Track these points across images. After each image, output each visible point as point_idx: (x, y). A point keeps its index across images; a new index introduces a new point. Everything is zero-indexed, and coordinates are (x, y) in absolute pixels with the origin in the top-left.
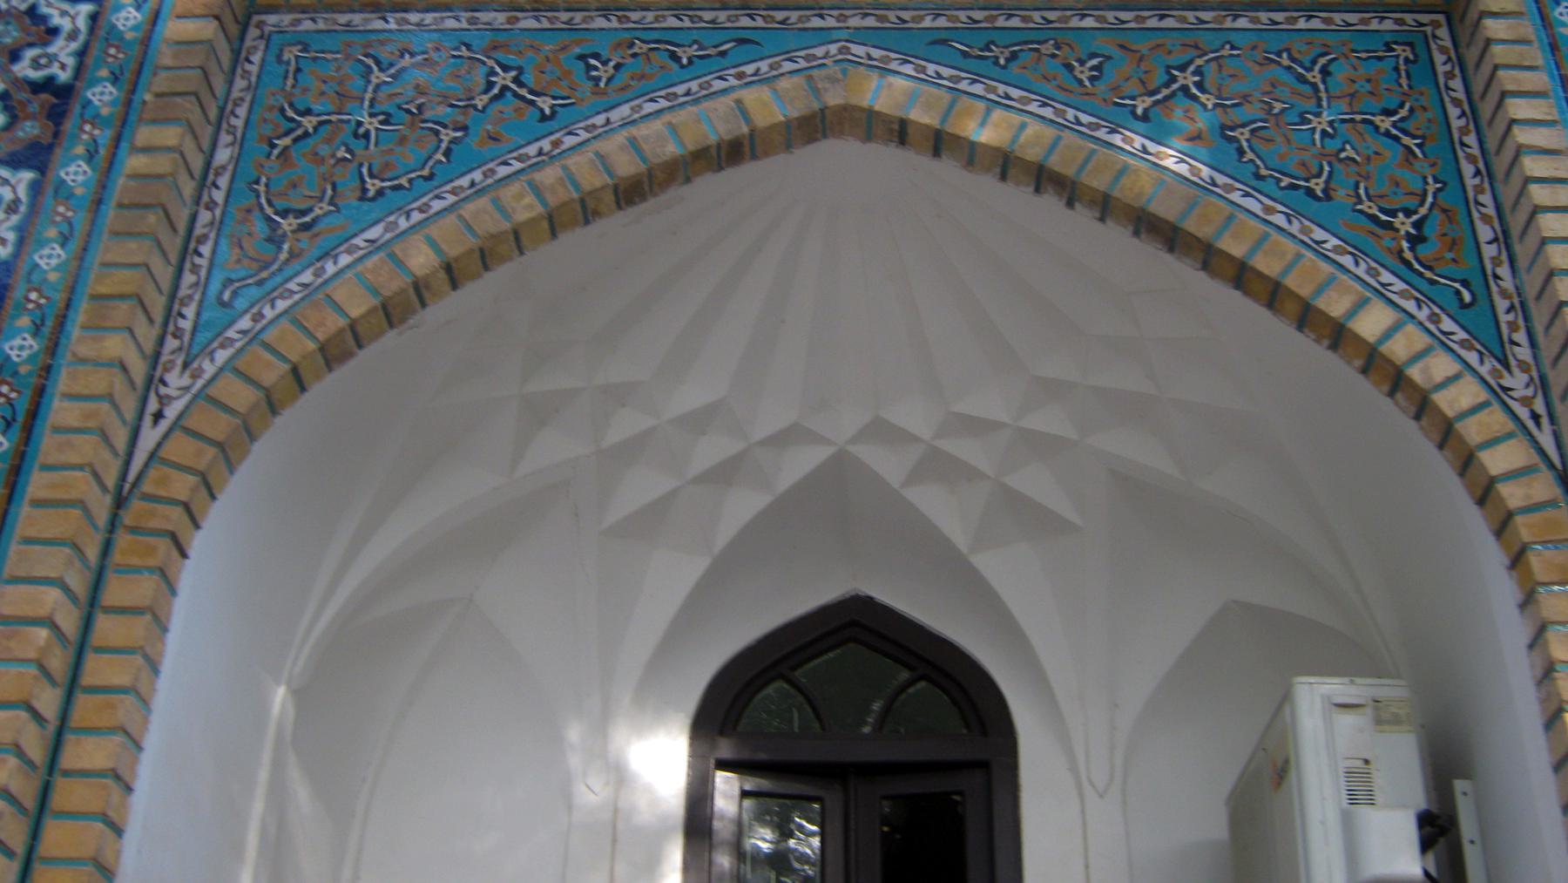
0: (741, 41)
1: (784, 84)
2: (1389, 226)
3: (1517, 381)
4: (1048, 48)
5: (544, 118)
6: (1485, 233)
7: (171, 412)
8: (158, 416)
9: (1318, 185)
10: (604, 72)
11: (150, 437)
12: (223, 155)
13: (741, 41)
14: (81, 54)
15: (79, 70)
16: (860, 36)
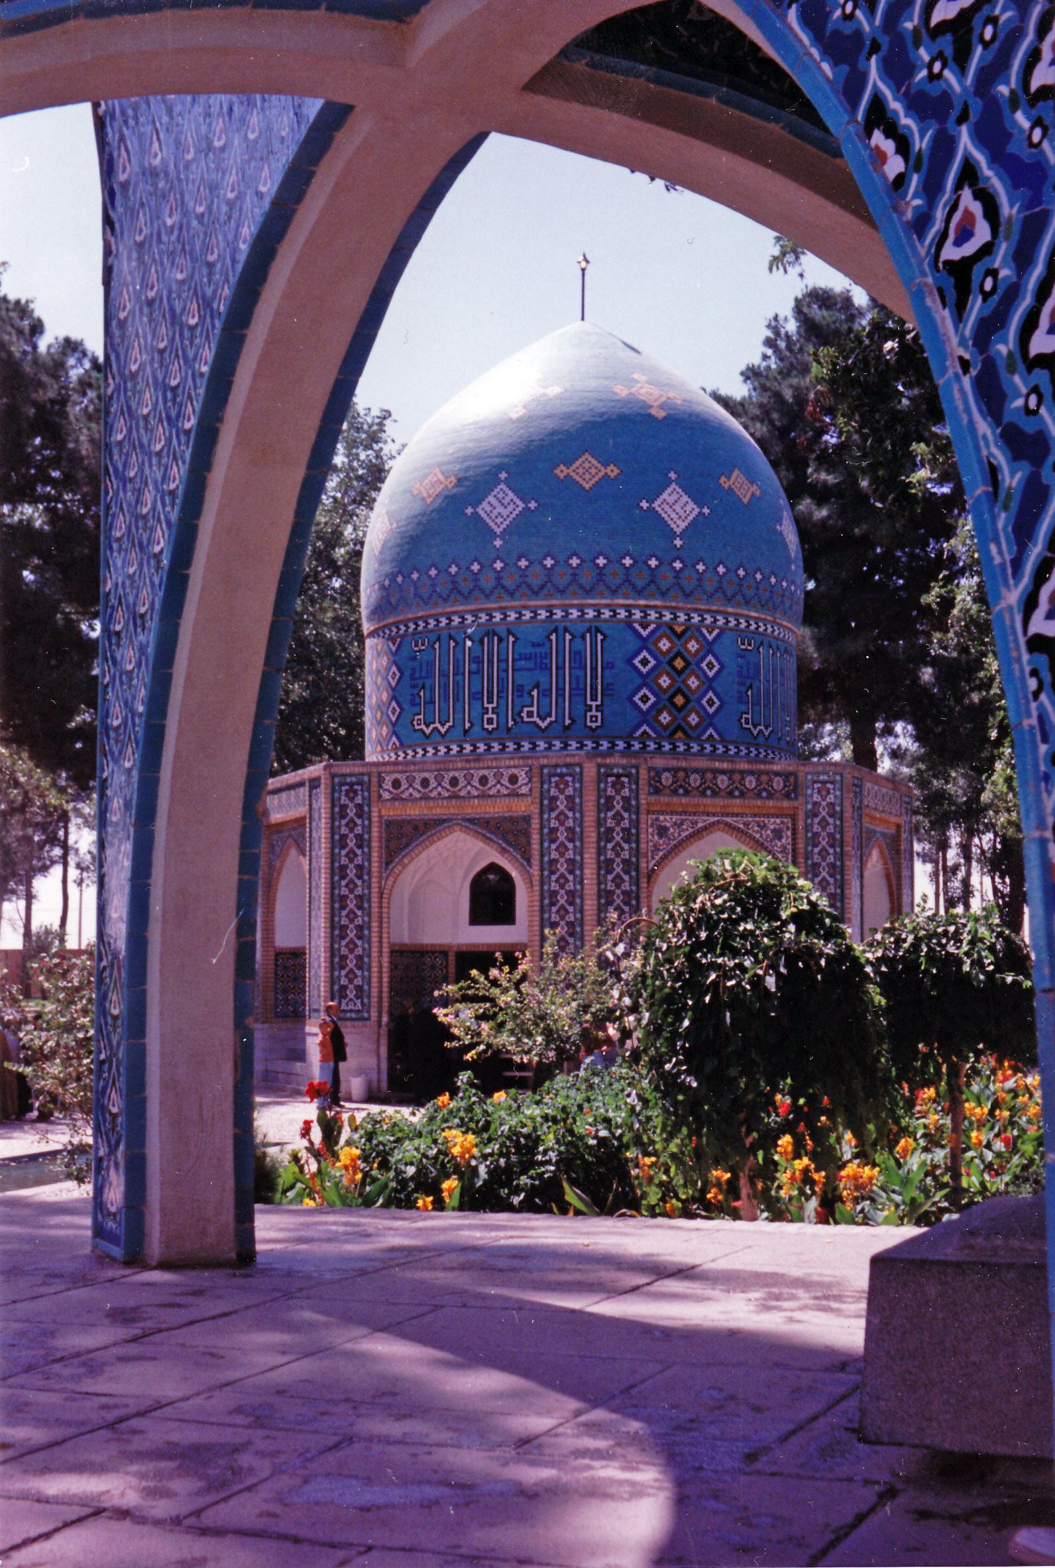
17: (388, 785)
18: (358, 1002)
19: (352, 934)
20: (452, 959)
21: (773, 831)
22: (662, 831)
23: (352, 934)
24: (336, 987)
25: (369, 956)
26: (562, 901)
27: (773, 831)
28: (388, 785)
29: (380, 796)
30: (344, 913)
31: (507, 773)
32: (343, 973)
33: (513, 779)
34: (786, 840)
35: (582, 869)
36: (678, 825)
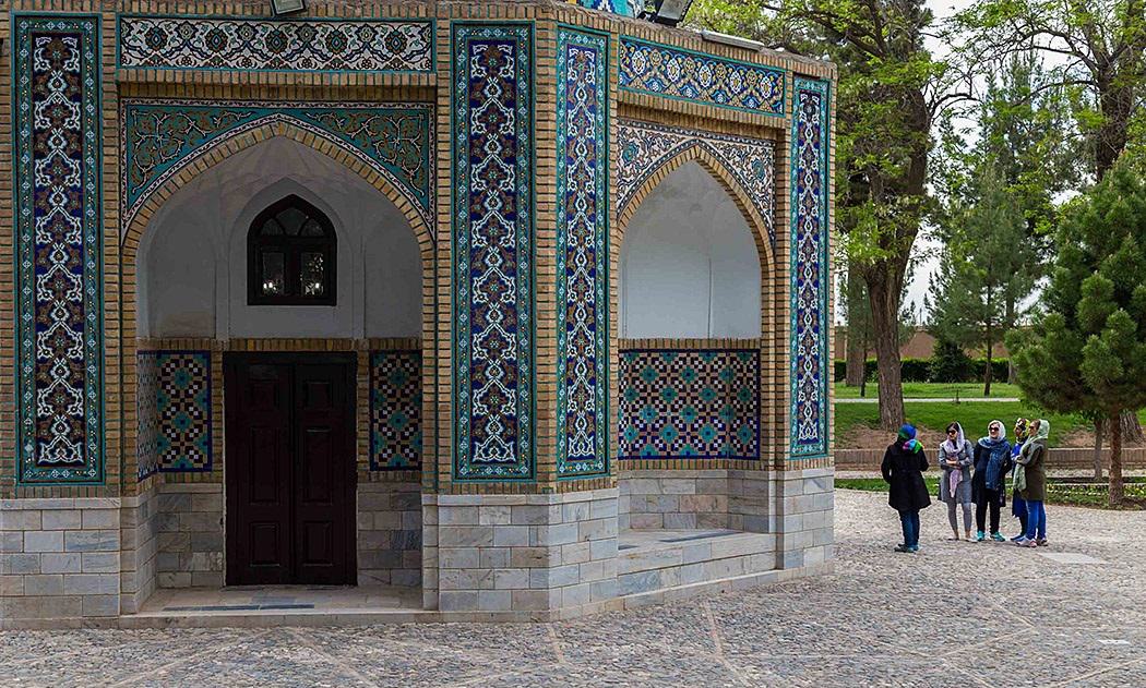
0: (253, 112)
1: (263, 127)
2: (408, 174)
3: (430, 218)
4: (331, 116)
5: (204, 138)
6: (431, 175)
7: (128, 224)
8: (125, 226)
9: (393, 161)
10: (218, 122)
11: (124, 232)
12: (123, 148)
13: (253, 112)
14: (80, 120)
15: (81, 125)
16: (283, 111)
17: (138, 35)
18: (77, 448)
19: (60, 320)
20: (217, 367)
21: (756, 164)
22: (629, 151)
23: (60, 320)
24: (29, 421)
25: (100, 363)
26: (493, 268)
27: (756, 164)
28: (138, 35)
29: (121, 58)
30: (43, 279)
31: (383, 32)
32: (43, 394)
33: (396, 42)
34: (767, 181)
35: (531, 208)
36: (647, 144)
